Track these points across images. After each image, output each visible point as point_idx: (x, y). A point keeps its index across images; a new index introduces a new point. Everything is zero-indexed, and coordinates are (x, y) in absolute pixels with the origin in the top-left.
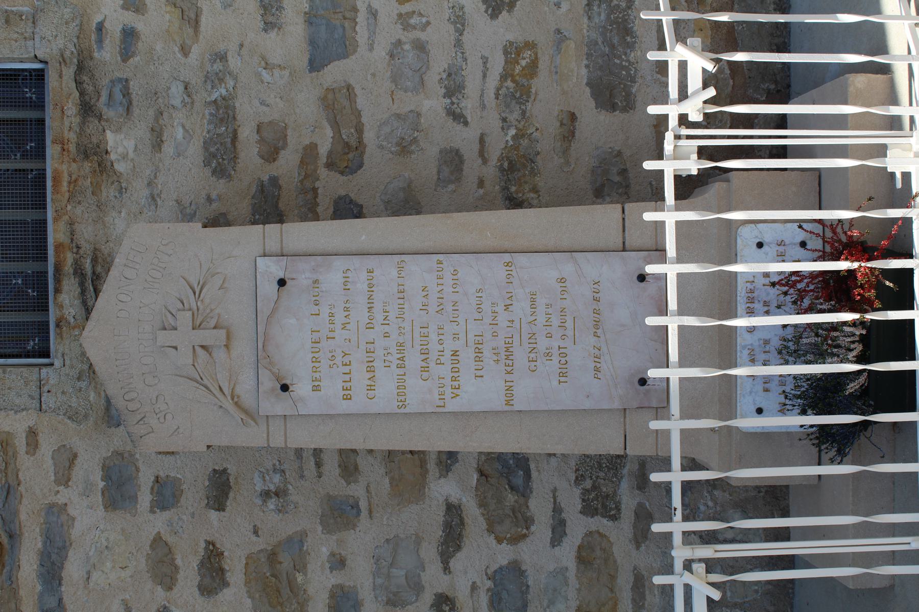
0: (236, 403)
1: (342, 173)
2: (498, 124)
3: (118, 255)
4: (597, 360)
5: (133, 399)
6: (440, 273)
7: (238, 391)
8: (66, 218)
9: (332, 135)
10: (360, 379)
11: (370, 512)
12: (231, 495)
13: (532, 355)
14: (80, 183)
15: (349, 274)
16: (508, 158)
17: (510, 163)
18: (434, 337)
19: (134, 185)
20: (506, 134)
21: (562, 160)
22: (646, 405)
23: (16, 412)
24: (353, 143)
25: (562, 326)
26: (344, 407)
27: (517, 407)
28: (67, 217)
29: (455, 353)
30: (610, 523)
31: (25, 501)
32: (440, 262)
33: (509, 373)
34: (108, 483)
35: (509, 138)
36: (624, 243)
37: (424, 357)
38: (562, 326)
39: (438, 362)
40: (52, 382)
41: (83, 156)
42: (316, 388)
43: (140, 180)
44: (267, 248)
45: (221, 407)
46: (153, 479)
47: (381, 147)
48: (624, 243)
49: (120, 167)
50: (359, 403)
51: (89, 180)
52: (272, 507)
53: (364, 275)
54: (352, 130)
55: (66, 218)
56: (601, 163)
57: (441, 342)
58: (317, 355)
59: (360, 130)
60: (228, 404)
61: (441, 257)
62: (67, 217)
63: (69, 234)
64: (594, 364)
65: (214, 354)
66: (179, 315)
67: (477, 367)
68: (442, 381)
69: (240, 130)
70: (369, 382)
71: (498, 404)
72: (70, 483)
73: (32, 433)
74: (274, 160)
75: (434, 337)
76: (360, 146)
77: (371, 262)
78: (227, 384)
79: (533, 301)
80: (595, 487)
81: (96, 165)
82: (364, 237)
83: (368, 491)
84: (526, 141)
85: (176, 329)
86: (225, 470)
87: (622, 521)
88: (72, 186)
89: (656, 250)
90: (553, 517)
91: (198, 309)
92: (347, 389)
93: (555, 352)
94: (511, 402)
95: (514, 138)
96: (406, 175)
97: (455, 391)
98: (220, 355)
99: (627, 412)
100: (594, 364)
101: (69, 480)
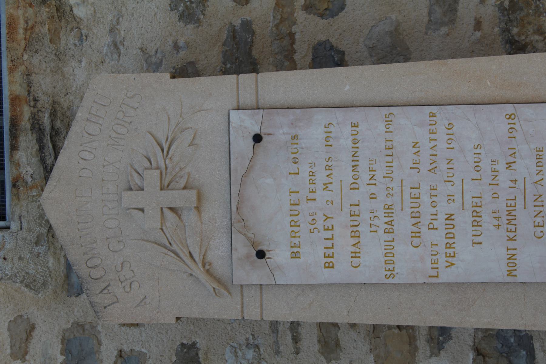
0: (208, 271)
1: (322, 16)
5: (96, 266)
6: (433, 127)
7: (210, 257)
8: (22, 68)
10: (344, 244)
13: (538, 220)
14: (37, 30)
15: (331, 129)
18: (426, 199)
19: (95, 31)
26: (326, 276)
28: (23, 67)
29: (450, 217)
32: (433, 115)
33: (511, 239)
34: (67, 358)
37: (414, 221)
39: (431, 226)
42: (295, 255)
43: (101, 26)
44: (241, 101)
45: (191, 275)
46: (116, 353)
49: (80, 12)
50: (342, 272)
51: (47, 26)
53: (348, 130)
55: (22, 68)
57: (433, 204)
60: (199, 272)
61: (434, 109)
62: (23, 67)
63: (25, 86)
65: (184, 217)
66: (147, 174)
67: (474, 233)
68: (435, 248)
70: (354, 249)
71: (499, 274)
72: (27, 357)
75: (426, 199)
77: (356, 115)
78: (198, 249)
81: (54, 10)
82: (347, 87)
85: (142, 190)
86: (194, 344)
88: (29, 33)
91: (166, 168)
92: (329, 257)
94: (514, 273)
96: (394, 17)
97: (450, 259)
98: (190, 218)
101: (26, 353)
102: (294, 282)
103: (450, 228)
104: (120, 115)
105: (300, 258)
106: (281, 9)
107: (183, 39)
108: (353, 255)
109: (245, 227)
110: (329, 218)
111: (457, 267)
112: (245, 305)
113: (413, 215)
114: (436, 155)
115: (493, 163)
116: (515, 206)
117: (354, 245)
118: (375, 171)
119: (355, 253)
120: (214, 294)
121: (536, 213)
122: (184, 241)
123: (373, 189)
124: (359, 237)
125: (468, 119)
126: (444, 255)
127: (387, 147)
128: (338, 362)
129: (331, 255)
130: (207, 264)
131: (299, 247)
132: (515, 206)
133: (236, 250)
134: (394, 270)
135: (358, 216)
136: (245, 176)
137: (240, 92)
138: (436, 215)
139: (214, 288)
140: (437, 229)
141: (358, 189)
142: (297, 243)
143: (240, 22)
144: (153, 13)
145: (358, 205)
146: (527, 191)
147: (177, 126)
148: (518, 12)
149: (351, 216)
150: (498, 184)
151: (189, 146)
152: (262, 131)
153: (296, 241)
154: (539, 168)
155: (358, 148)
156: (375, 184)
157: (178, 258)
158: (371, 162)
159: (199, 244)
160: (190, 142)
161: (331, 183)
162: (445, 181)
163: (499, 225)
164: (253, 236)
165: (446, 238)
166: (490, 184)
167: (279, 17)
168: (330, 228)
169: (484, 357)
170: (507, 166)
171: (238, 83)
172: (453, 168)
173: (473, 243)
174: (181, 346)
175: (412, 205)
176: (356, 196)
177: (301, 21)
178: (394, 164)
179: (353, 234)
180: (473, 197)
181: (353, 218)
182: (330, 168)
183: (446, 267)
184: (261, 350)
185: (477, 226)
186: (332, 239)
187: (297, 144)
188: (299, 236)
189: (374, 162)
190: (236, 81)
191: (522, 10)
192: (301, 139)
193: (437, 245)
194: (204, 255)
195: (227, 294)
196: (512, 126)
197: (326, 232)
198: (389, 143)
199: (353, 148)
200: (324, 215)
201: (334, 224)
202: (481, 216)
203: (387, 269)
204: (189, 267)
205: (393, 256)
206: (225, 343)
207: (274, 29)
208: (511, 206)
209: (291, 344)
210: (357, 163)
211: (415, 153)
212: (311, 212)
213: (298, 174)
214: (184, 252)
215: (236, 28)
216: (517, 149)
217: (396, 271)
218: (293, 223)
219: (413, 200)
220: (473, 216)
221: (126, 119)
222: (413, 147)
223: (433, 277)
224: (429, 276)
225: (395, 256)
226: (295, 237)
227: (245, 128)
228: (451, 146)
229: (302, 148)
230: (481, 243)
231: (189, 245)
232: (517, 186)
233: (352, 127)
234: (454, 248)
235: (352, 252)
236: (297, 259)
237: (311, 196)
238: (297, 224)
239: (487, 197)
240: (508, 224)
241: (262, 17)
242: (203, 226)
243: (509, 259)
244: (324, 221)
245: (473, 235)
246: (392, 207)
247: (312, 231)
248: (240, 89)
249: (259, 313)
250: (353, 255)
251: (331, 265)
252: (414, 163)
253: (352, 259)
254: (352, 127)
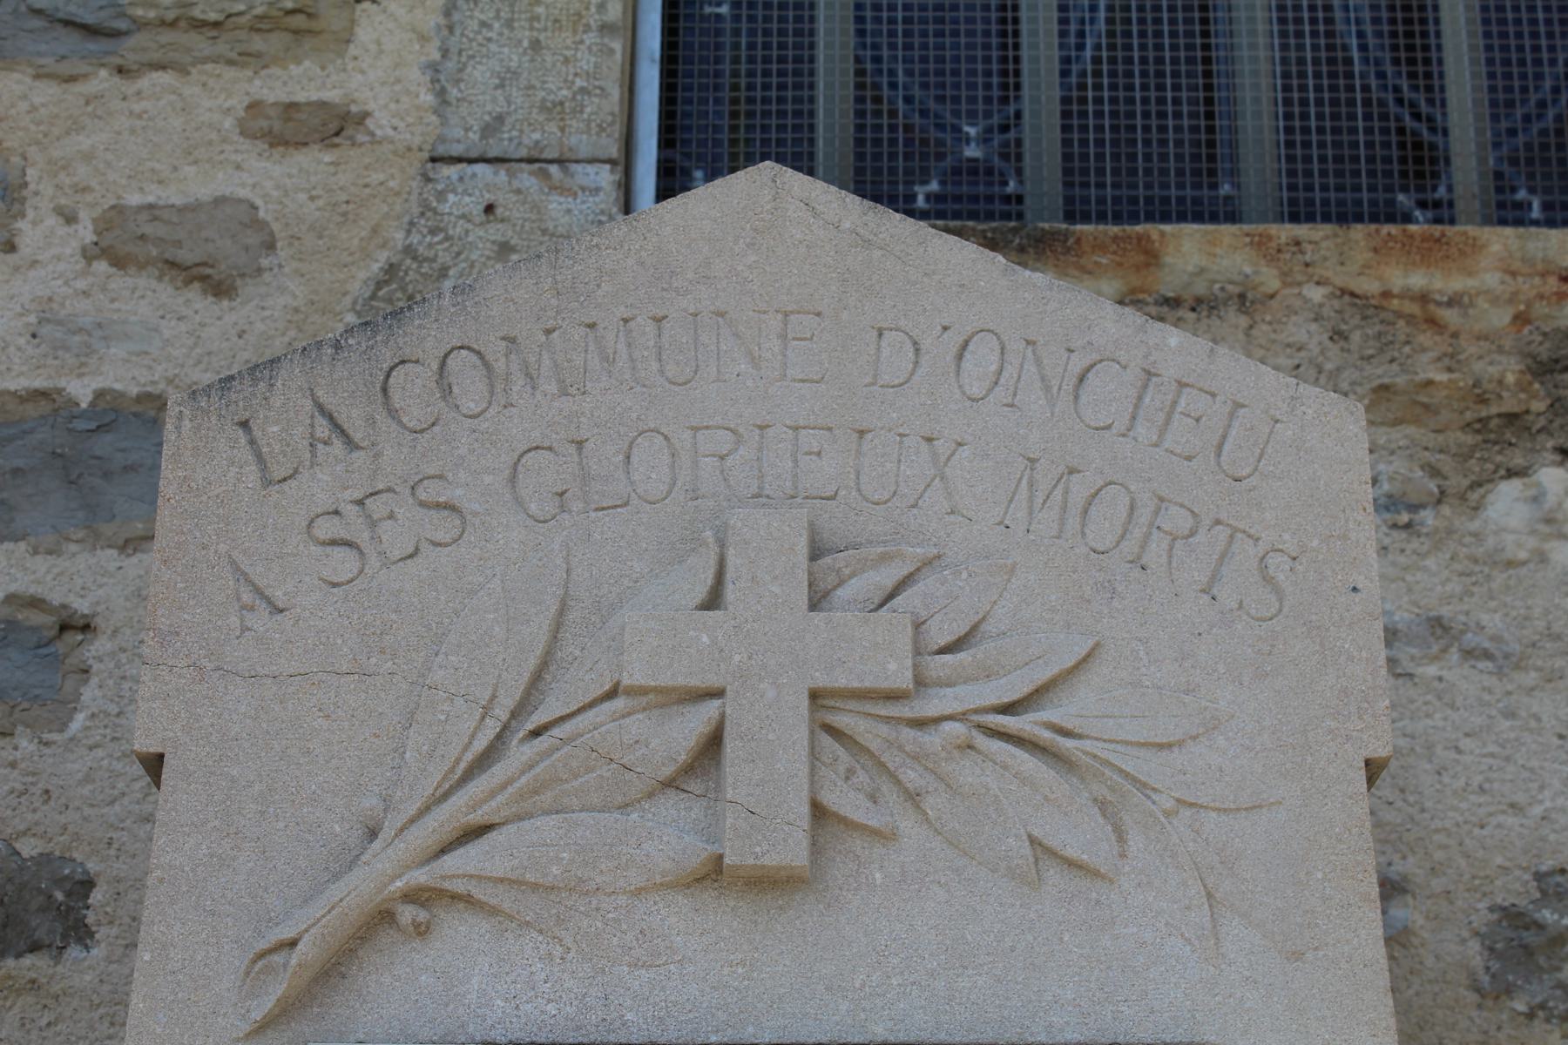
0: (384, 917)
3: (1203, 344)
5: (447, 391)
7: (457, 928)
8: (1269, 279)
14: (1425, 338)
19: (1430, 562)
23: (434, 68)
28: (1274, 284)
31: (46, 92)
34: (82, 415)
40: (555, 205)
41: (1544, 351)
43: (1455, 587)
45: (373, 834)
46: (82, 606)
49: (1506, 505)
51: (1442, 377)
55: (1269, 279)
60: (384, 870)
62: (1274, 284)
63: (1200, 288)
65: (670, 806)
66: (893, 627)
72: (102, 266)
73: (337, 126)
78: (499, 868)
81: (1510, 404)
85: (814, 606)
86: (81, 933)
88: (1413, 308)
91: (920, 724)
98: (669, 835)
101: (119, 262)
104: (1177, 519)
107: (1421, 922)
120: (263, 945)
122: (547, 798)
130: (423, 916)
139: (293, 944)
144: (1520, 798)
147: (1134, 780)
151: (1033, 840)
157: (463, 765)
159: (530, 877)
174: (78, 877)
194: (467, 900)
195: (257, 1015)
204: (412, 821)
214: (493, 794)
221: (1158, 545)
231: (526, 824)
242: (622, 900)
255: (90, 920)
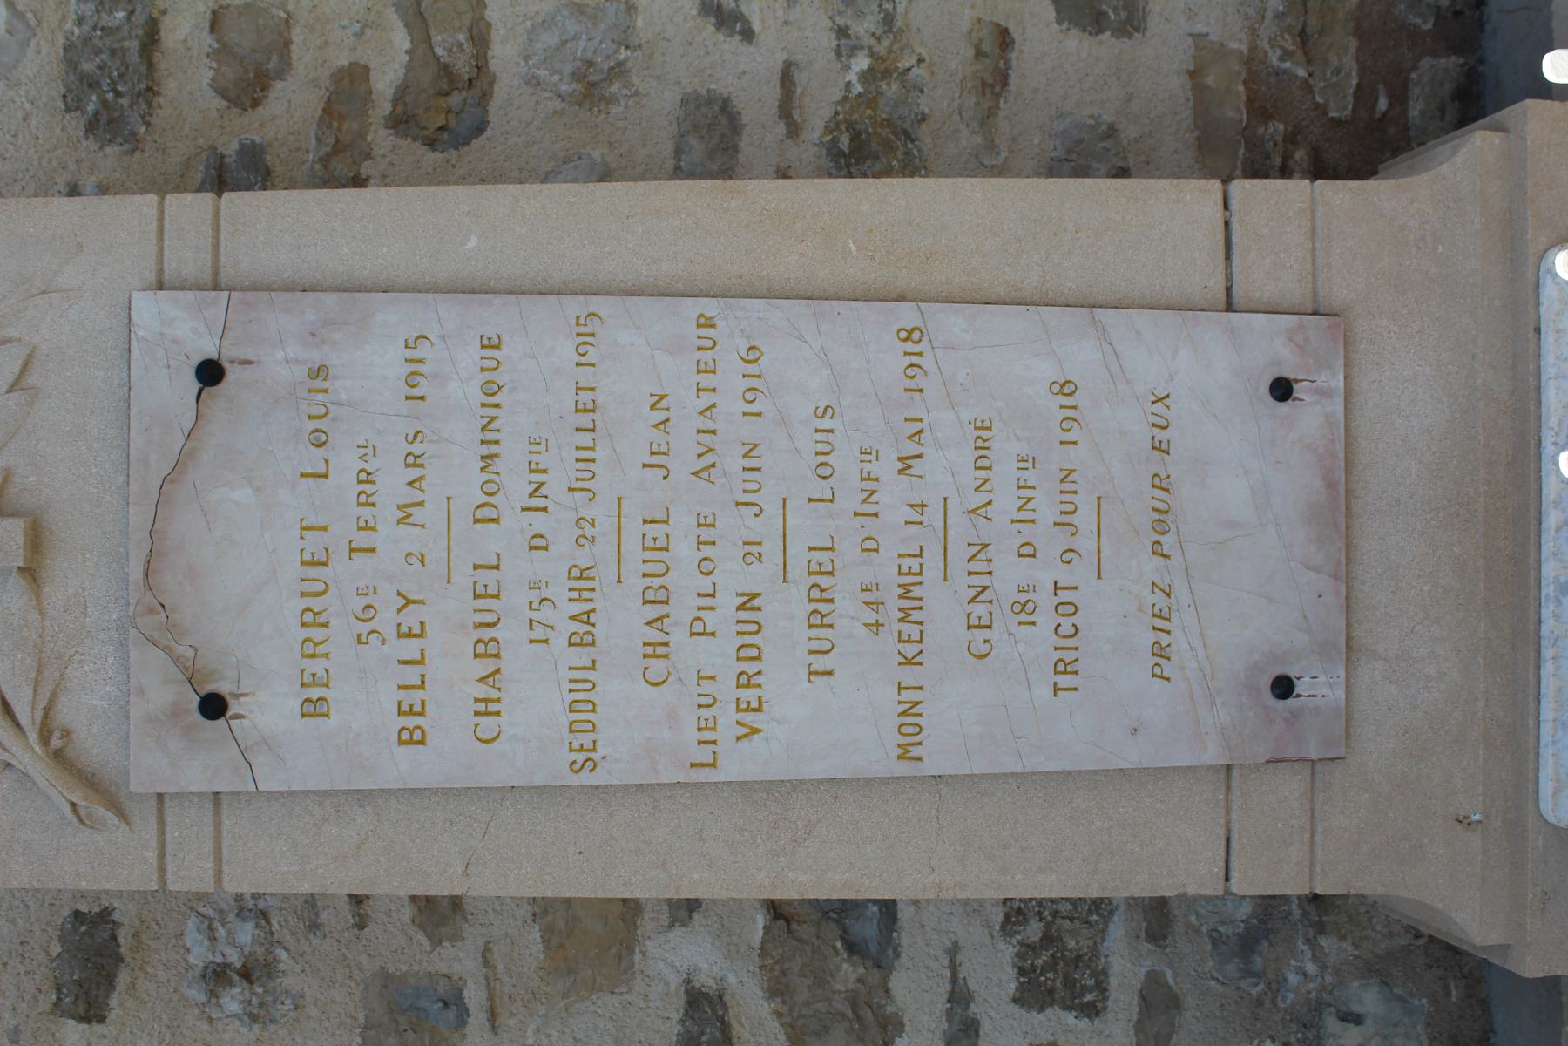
0: (58, 756)
1: (431, 144)
2: (828, 41)
4: (1160, 623)
6: (707, 356)
7: (67, 713)
9: (407, 45)
10: (453, 675)
11: (493, 1015)
12: (123, 978)
13: (979, 610)
15: (424, 351)
16: (850, 125)
17: (856, 137)
18: (684, 552)
20: (847, 68)
21: (979, 139)
22: (1291, 753)
24: (463, 68)
25: (1065, 523)
26: (402, 767)
27: (930, 767)
29: (749, 602)
30: (1083, 1024)
32: (706, 323)
33: (908, 662)
35: (852, 77)
36: (1229, 290)
37: (652, 612)
38: (1065, 523)
39: (698, 627)
42: (314, 709)
44: (170, 267)
45: (8, 765)
47: (533, 82)
48: (1229, 290)
50: (448, 757)
52: (234, 1008)
53: (470, 355)
54: (462, 37)
56: (1069, 151)
57: (705, 566)
58: (316, 604)
59: (480, 38)
61: (710, 307)
64: (1152, 637)
67: (815, 645)
68: (707, 687)
69: (166, 23)
70: (482, 691)
71: (873, 752)
74: (256, 103)
75: (684, 552)
76: (479, 80)
77: (496, 315)
78: (27, 692)
79: (982, 446)
80: (1048, 939)
82: (473, 242)
83: (486, 963)
84: (894, 87)
86: (106, 913)
87: (1110, 1016)
89: (1314, 313)
90: (950, 1014)
92: (411, 712)
93: (1045, 599)
94: (916, 751)
95: (865, 77)
96: (597, 155)
97: (749, 718)
99: (1235, 773)
100: (1152, 637)
102: (312, 785)
103: (751, 633)
105: (327, 716)
106: (335, 124)
108: (481, 707)
109: (169, 626)
110: (414, 602)
111: (767, 739)
112: (169, 849)
113: (650, 595)
114: (714, 432)
115: (864, 457)
116: (920, 574)
117: (482, 680)
118: (545, 471)
119: (486, 701)
120: (75, 820)
121: (973, 592)
123: (539, 522)
124: (497, 656)
125: (801, 338)
126: (734, 706)
127: (580, 406)
128: (459, 944)
129: (417, 708)
130: (57, 734)
131: (327, 686)
132: (920, 574)
133: (141, 692)
134: (594, 750)
135: (497, 596)
136: (172, 481)
137: (166, 243)
138: (713, 596)
139: (73, 805)
140: (713, 634)
141: (495, 520)
142: (321, 673)
143: (237, 146)
144: (20, 115)
145: (497, 567)
146: (951, 533)
148: (869, 162)
149: (476, 596)
150: (876, 515)
151: (10, 391)
152: (223, 351)
153: (318, 667)
154: (983, 474)
155: (497, 406)
156: (545, 509)
158: (535, 448)
159: (33, 675)
160: (11, 380)
161: (420, 504)
162: (738, 504)
163: (878, 624)
164: (191, 653)
165: (738, 659)
166: (856, 514)
167: (331, 140)
168: (416, 630)
169: (787, 921)
170: (900, 465)
171: (161, 219)
172: (758, 469)
173: (810, 673)
175: (649, 568)
176: (490, 542)
177: (382, 152)
178: (596, 454)
179: (481, 648)
180: (811, 549)
181: (480, 603)
182: (419, 461)
183: (738, 738)
184: (274, 922)
185: (823, 626)
186: (421, 662)
187: (325, 391)
188: (327, 655)
189: (542, 448)
190: (154, 211)
191: (877, 157)
192: (336, 378)
193: (713, 678)
194: (47, 711)
195: (116, 820)
196: (915, 359)
197: (405, 641)
198: (586, 397)
199: (483, 405)
200: (399, 594)
201: (426, 619)
202: (831, 601)
203: (575, 745)
205: (593, 711)
206: (184, 909)
207: (318, 166)
208: (909, 573)
209: (347, 907)
210: (494, 449)
211: (656, 426)
212: (362, 584)
213: (325, 476)
215: (227, 160)
216: (926, 421)
217: (601, 751)
218: (308, 617)
219: (648, 555)
220: (811, 601)
222: (653, 407)
223: (702, 765)
224: (692, 765)
225: (598, 709)
226: (313, 656)
227: (175, 342)
228: (754, 408)
229: (338, 404)
230: (830, 673)
232: (924, 519)
233: (483, 347)
234: (759, 686)
235: (476, 700)
236: (321, 719)
237: (362, 540)
238: (322, 619)
239: (848, 549)
240: (901, 620)
241: (291, 138)
242: (47, 623)
243: (904, 713)
244: (400, 610)
245: (812, 652)
246: (592, 573)
247: (363, 639)
248: (166, 237)
249: (211, 872)
250: (481, 707)
251: (417, 735)
252: (652, 453)
253: (479, 719)
254: (483, 347)
255: (97, 910)
